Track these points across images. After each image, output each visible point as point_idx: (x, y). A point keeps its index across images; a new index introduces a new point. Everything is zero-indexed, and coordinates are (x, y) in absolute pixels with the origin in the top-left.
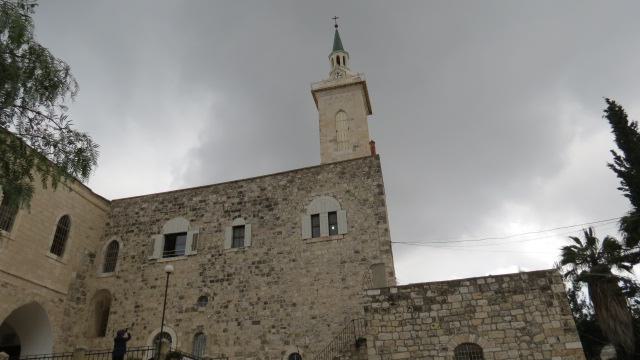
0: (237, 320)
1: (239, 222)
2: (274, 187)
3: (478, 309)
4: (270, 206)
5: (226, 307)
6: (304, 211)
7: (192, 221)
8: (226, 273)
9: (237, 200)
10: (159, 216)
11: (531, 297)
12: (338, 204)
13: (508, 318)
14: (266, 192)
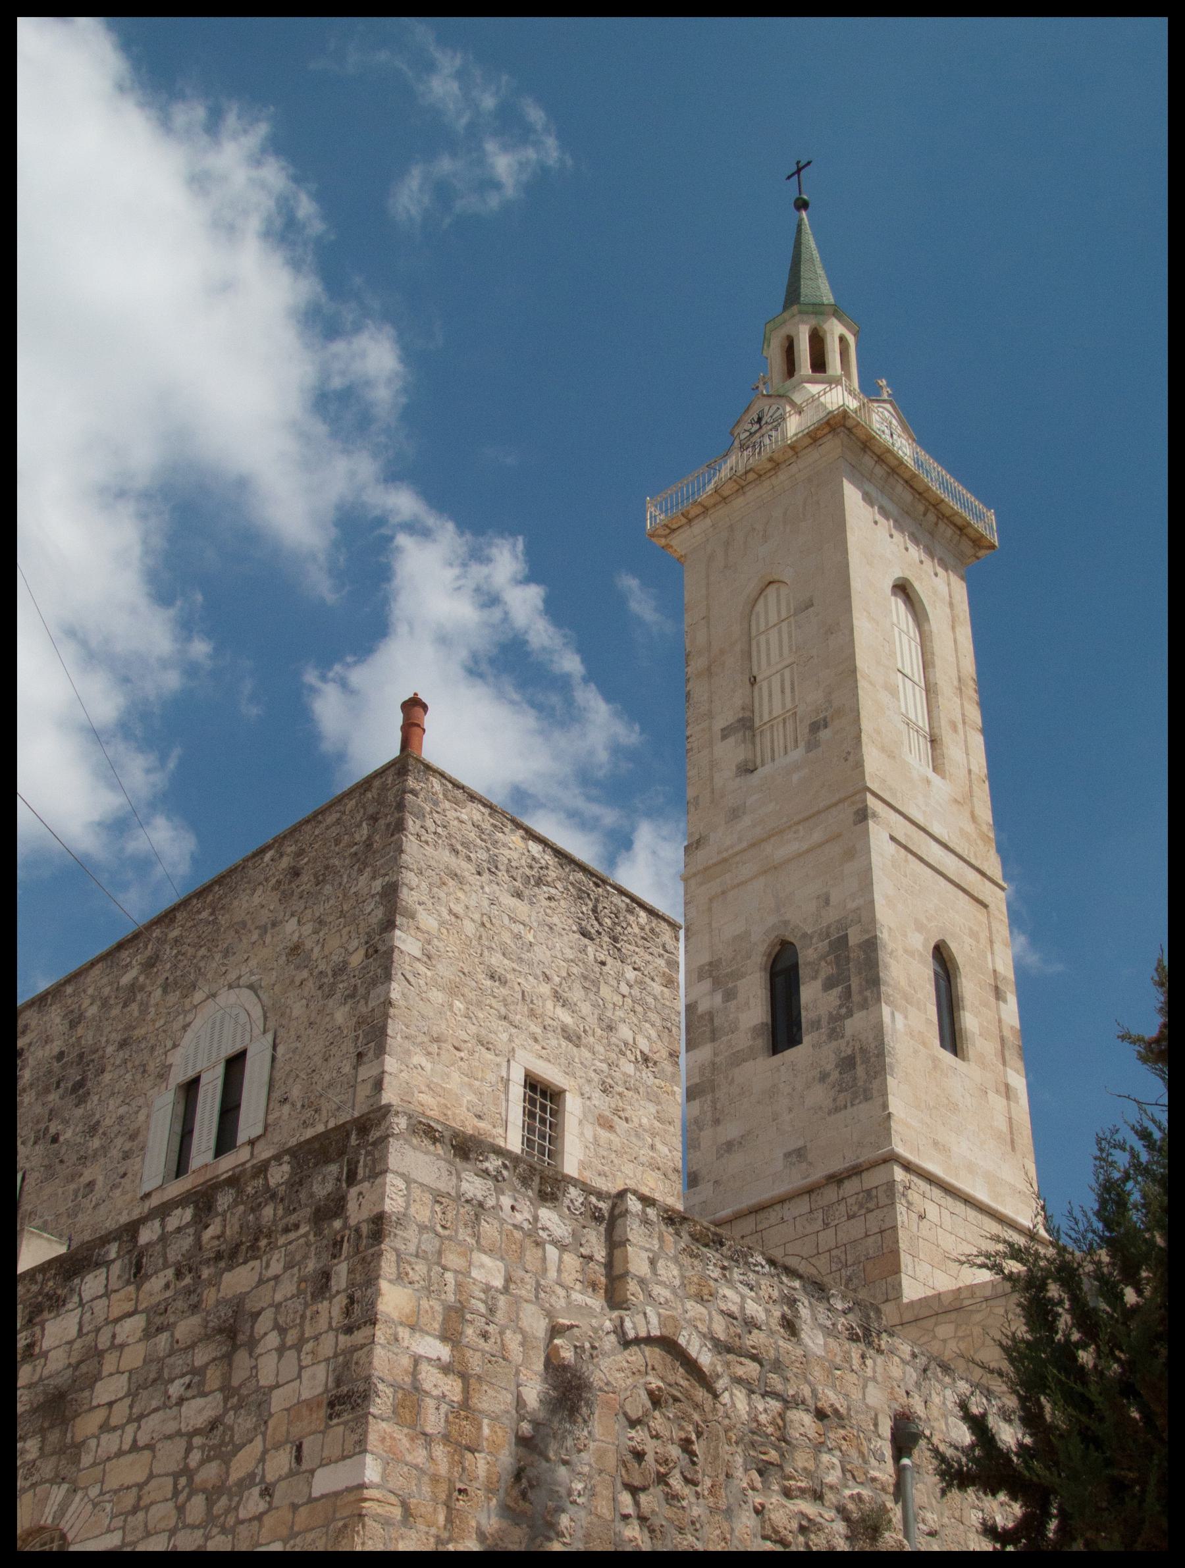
2: (105, 1004)
6: (163, 1074)
11: (276, 1268)
12: (257, 1012)
14: (80, 1031)
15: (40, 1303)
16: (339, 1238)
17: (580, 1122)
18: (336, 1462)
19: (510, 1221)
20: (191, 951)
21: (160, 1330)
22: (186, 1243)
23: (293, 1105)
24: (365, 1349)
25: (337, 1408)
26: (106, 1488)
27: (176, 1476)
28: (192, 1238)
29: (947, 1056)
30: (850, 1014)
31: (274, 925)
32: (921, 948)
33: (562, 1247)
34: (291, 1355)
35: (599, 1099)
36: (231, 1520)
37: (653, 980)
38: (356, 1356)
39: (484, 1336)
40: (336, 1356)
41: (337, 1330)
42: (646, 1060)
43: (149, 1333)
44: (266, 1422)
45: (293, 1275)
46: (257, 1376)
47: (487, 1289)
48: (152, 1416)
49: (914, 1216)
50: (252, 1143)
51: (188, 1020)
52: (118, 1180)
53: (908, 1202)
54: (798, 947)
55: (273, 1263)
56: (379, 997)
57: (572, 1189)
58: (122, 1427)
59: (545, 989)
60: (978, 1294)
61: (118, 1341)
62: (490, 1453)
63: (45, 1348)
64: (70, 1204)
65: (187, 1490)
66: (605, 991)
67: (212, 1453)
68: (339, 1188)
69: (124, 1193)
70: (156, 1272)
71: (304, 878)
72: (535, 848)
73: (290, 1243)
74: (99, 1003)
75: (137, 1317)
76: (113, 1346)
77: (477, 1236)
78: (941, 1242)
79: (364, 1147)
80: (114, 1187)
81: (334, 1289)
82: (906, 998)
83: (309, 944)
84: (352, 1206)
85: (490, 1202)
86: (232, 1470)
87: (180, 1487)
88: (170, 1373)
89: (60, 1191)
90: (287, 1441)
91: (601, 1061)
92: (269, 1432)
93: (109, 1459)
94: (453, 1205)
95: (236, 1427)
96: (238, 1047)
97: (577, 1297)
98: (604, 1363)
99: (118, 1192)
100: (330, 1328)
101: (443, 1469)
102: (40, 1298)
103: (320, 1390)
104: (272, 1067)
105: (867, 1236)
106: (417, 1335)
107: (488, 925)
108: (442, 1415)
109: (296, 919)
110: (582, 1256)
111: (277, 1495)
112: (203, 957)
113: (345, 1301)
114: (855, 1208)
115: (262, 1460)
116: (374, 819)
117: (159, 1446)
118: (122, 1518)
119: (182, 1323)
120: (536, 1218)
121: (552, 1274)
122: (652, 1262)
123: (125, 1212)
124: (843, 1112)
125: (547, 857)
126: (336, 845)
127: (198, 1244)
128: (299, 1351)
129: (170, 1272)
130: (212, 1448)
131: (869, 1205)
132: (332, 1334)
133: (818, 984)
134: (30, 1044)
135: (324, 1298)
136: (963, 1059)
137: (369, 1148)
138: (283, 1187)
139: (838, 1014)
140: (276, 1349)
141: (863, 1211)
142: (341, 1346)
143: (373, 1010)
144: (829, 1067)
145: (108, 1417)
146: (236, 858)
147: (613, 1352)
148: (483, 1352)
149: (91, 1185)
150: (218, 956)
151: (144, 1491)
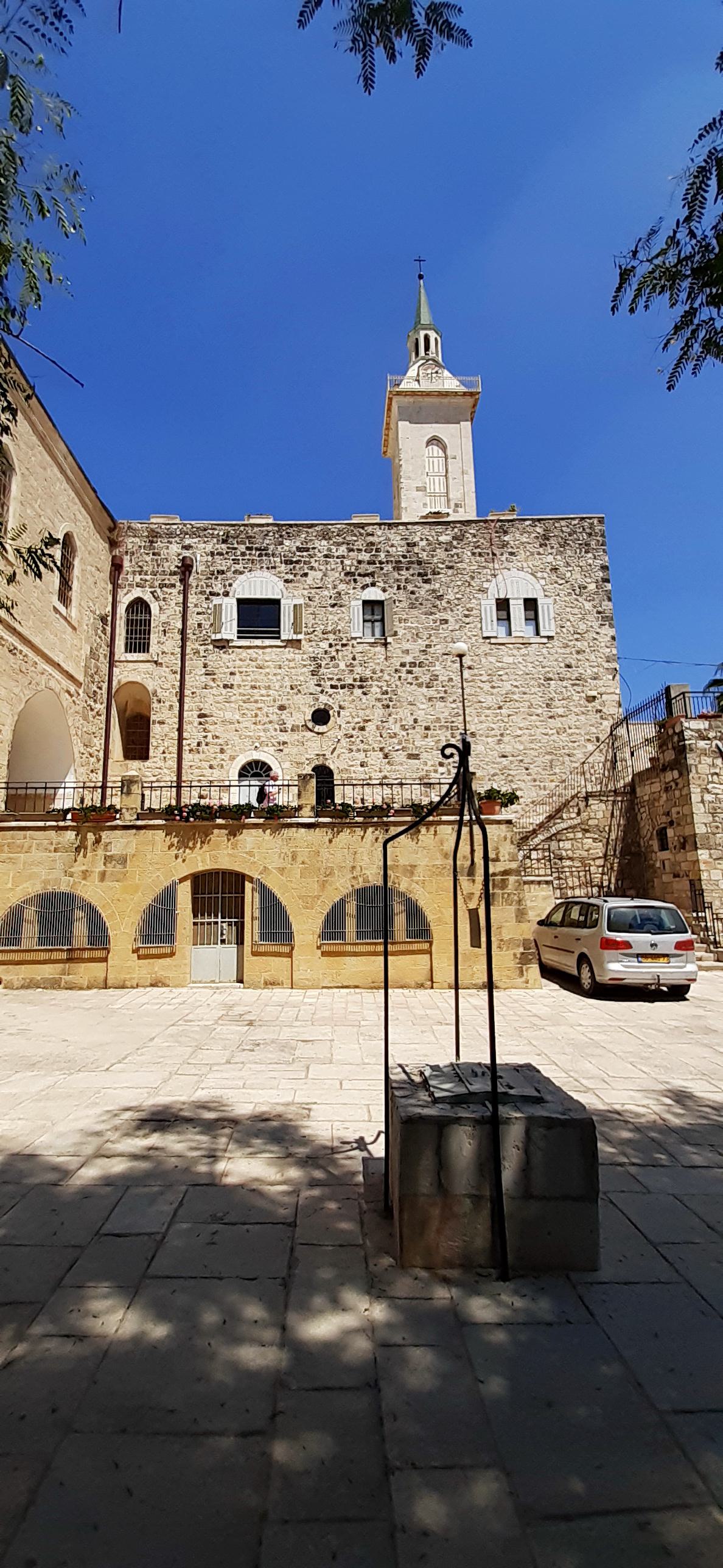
0: (381, 749)
1: (374, 594)
5: (362, 729)
8: (358, 677)
10: (221, 564)
12: (538, 587)
14: (416, 550)
71: (553, 541)
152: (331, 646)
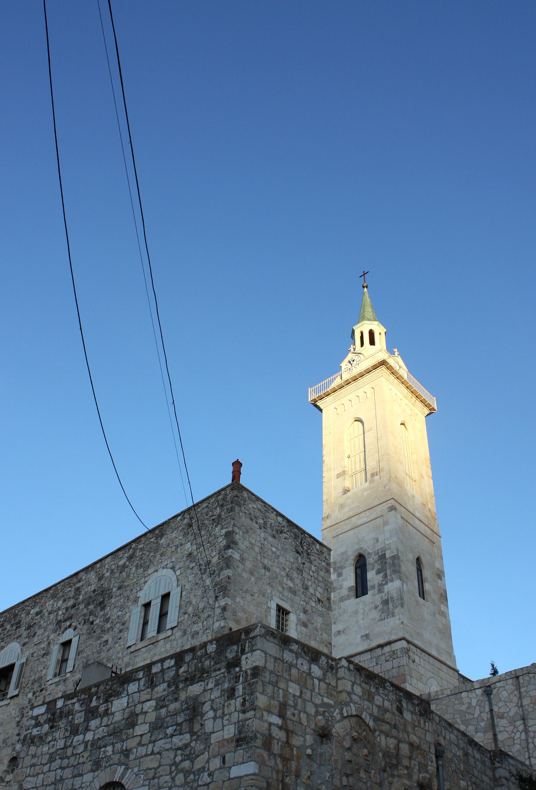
1: (68, 634)
2: (112, 571)
3: (141, 719)
4: (102, 602)
6: (136, 600)
7: (24, 645)
9: (71, 603)
12: (174, 578)
13: (170, 731)
14: (102, 582)
15: (111, 693)
16: (238, 675)
17: (296, 625)
18: (240, 764)
19: (301, 669)
20: (147, 553)
21: (162, 707)
22: (172, 673)
23: (189, 615)
24: (251, 720)
25: (240, 743)
26: (141, 769)
27: (171, 766)
28: (174, 672)
29: (421, 600)
30: (386, 583)
31: (181, 545)
32: (412, 559)
33: (320, 680)
34: (219, 721)
35: (302, 616)
36: (195, 785)
37: (321, 570)
38: (247, 722)
39: (293, 715)
40: (238, 722)
41: (238, 712)
42: (319, 600)
43: (158, 708)
44: (209, 747)
45: (219, 689)
46: (204, 728)
47: (294, 696)
48: (160, 741)
49: (411, 661)
50: (172, 629)
51: (146, 579)
52: (117, 640)
53: (409, 656)
54: (366, 557)
55: (210, 684)
56: (224, 575)
57: (323, 657)
58: (147, 745)
59: (283, 573)
60: (445, 693)
61: (144, 711)
62: (296, 761)
63: (113, 710)
64: (98, 649)
65: (175, 772)
66: (305, 574)
67: (186, 758)
68: (237, 656)
69: (120, 646)
70: (159, 684)
72: (280, 519)
73: (217, 676)
74: (110, 571)
75: (152, 702)
76: (142, 713)
77: (290, 675)
78: (420, 671)
79: (248, 640)
80: (116, 643)
81: (237, 695)
82: (407, 578)
83: (195, 553)
84: (243, 662)
85: (295, 662)
86: (194, 765)
87: (172, 770)
88: (167, 725)
89: (94, 643)
90: (219, 755)
91: (303, 601)
92: (210, 751)
93: (142, 757)
94: (281, 663)
95: (196, 748)
96: (167, 591)
97: (326, 700)
98: (337, 726)
99: (117, 645)
100: (236, 710)
101: (280, 767)
102: (110, 692)
103: (232, 735)
104: (181, 600)
105: (393, 668)
106: (270, 715)
107: (263, 548)
108: (280, 746)
109: (190, 543)
110: (327, 683)
111: (215, 776)
112: (152, 556)
113: (242, 701)
114: (389, 658)
115: (208, 762)
116: (222, 506)
117: (163, 753)
118: (149, 781)
119: (171, 705)
120: (310, 668)
121: (317, 690)
122: (353, 686)
123: (120, 653)
124: (384, 621)
125: (284, 523)
126: (206, 516)
127: (177, 675)
128: (223, 719)
129: (165, 685)
130: (185, 756)
131: (394, 657)
132: (236, 713)
133: (374, 572)
134: (82, 586)
135: (232, 699)
136: (427, 601)
137: (250, 640)
138: (214, 653)
139: (382, 583)
140: (213, 718)
141: (392, 659)
142: (241, 718)
143: (222, 580)
144: (379, 603)
145: (141, 740)
146: (166, 519)
147: (339, 722)
148: (293, 721)
149: (107, 641)
150: (158, 556)
151: (157, 771)
152: (34, 693)
